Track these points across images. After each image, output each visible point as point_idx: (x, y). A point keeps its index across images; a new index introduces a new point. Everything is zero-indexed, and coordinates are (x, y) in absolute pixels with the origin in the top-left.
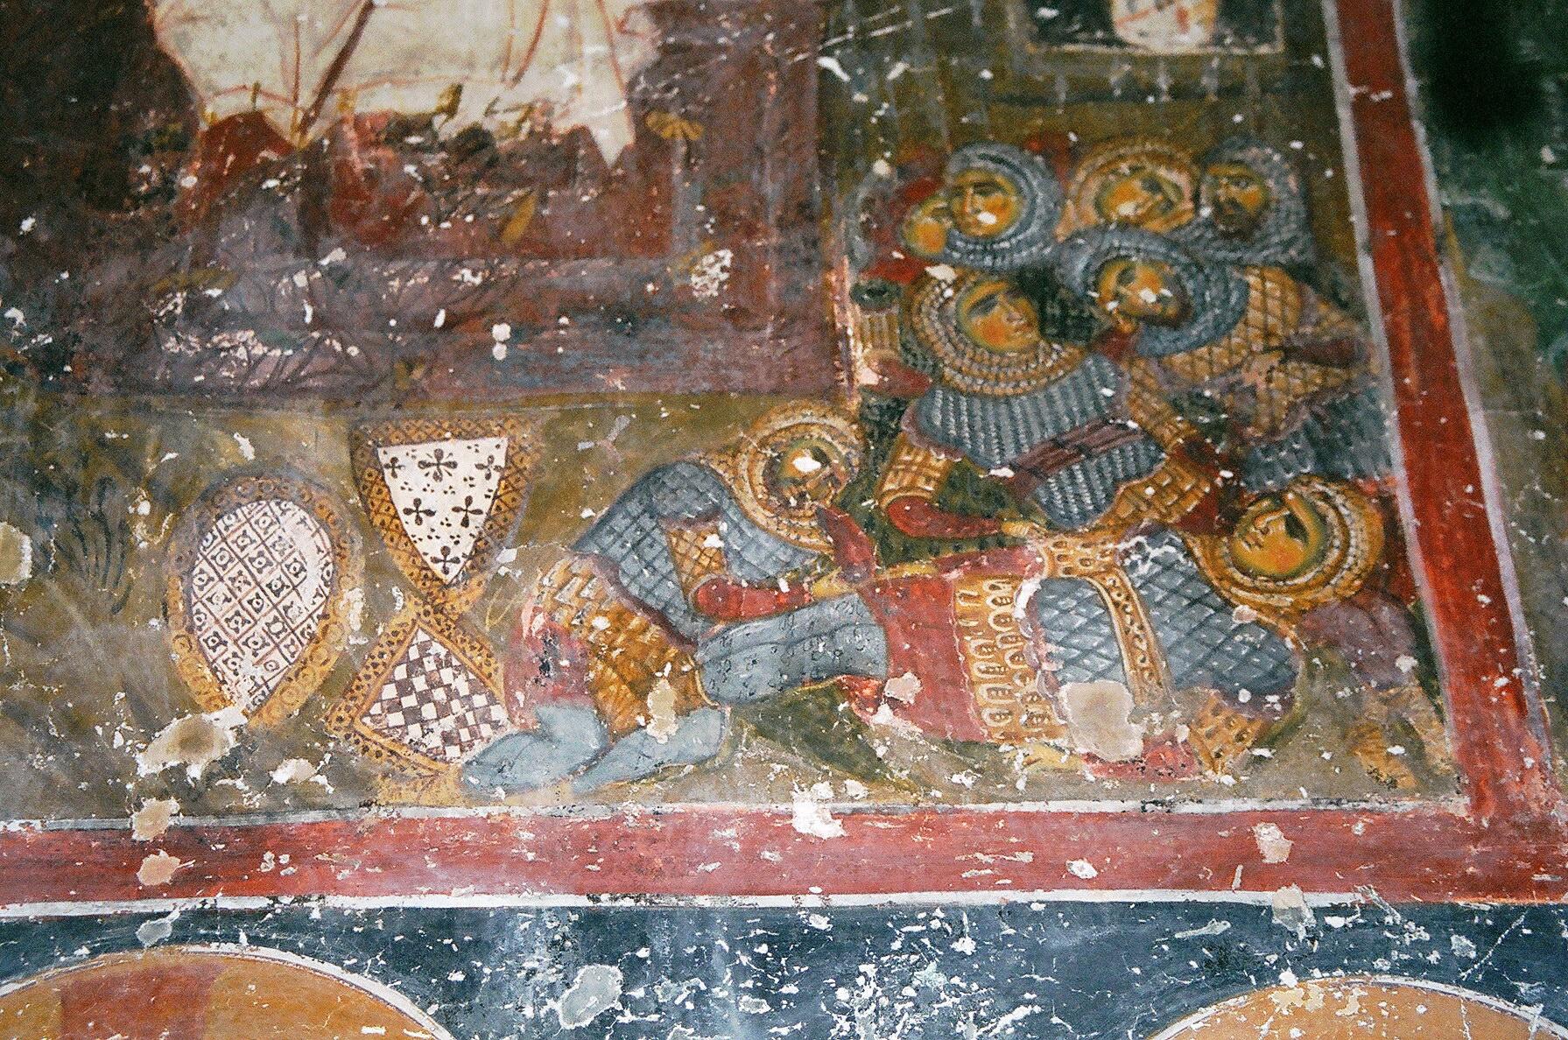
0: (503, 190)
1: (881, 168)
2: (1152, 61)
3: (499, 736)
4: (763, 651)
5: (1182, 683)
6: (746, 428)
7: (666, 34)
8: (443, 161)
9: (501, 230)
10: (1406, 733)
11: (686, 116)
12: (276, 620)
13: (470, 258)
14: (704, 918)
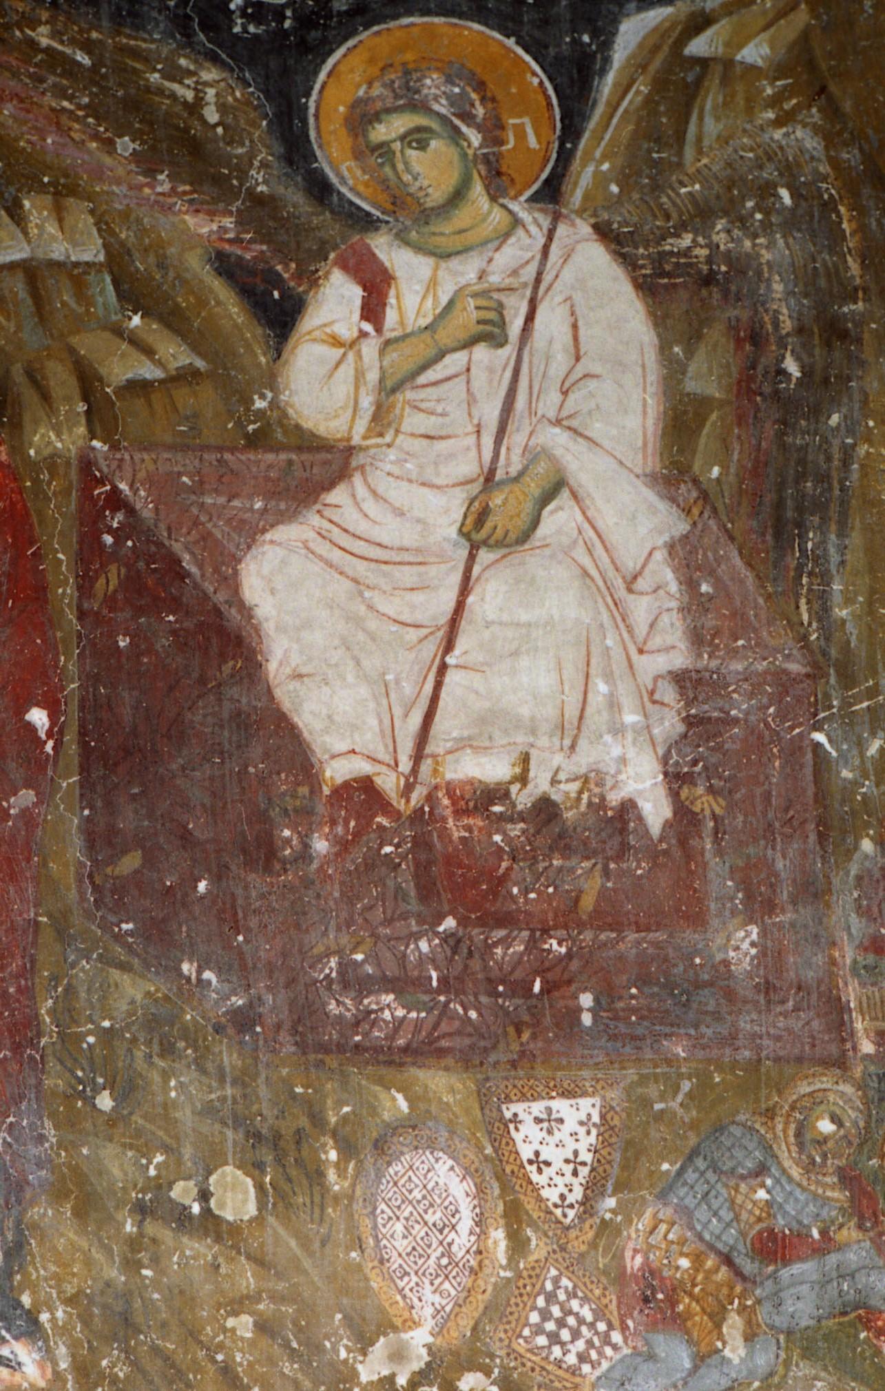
0: (573, 862)
1: (867, 845)
3: (618, 1357)
4: (805, 1289)
6: (780, 1093)
7: (688, 704)
8: (524, 832)
9: (577, 900)
11: (711, 790)
12: (443, 1255)
13: (555, 928)
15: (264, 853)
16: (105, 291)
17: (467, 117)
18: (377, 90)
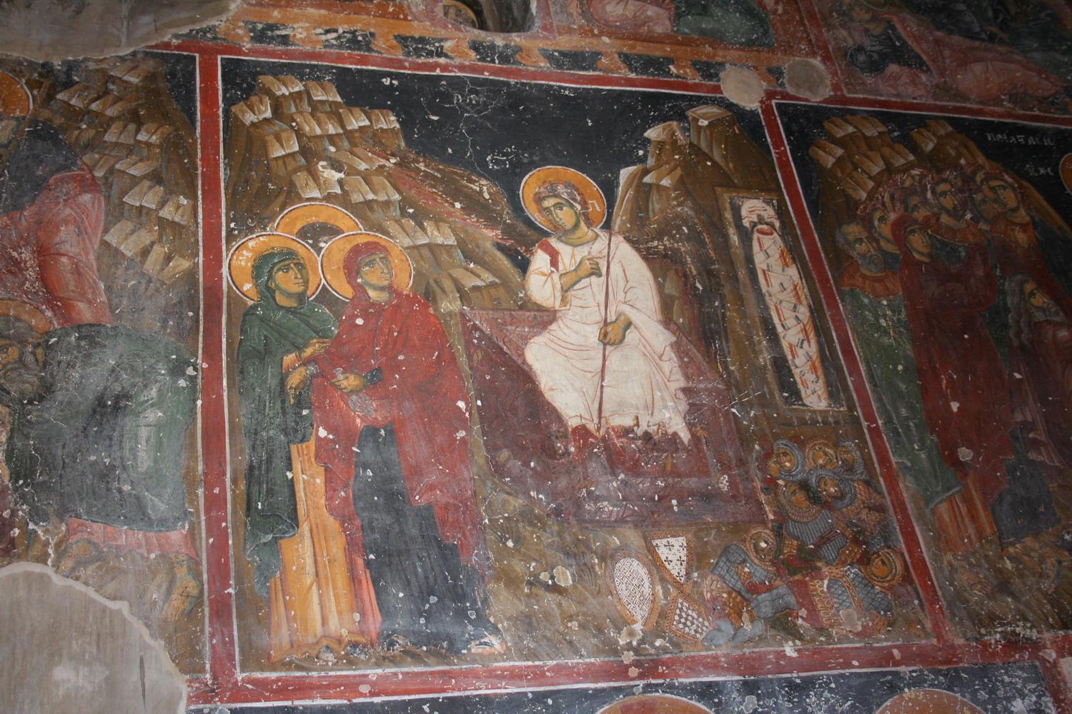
1: (757, 447)
2: (814, 412)
5: (867, 610)
7: (689, 399)
10: (920, 622)
14: (771, 680)
15: (553, 454)
16: (459, 255)
17: (575, 200)
18: (542, 190)
